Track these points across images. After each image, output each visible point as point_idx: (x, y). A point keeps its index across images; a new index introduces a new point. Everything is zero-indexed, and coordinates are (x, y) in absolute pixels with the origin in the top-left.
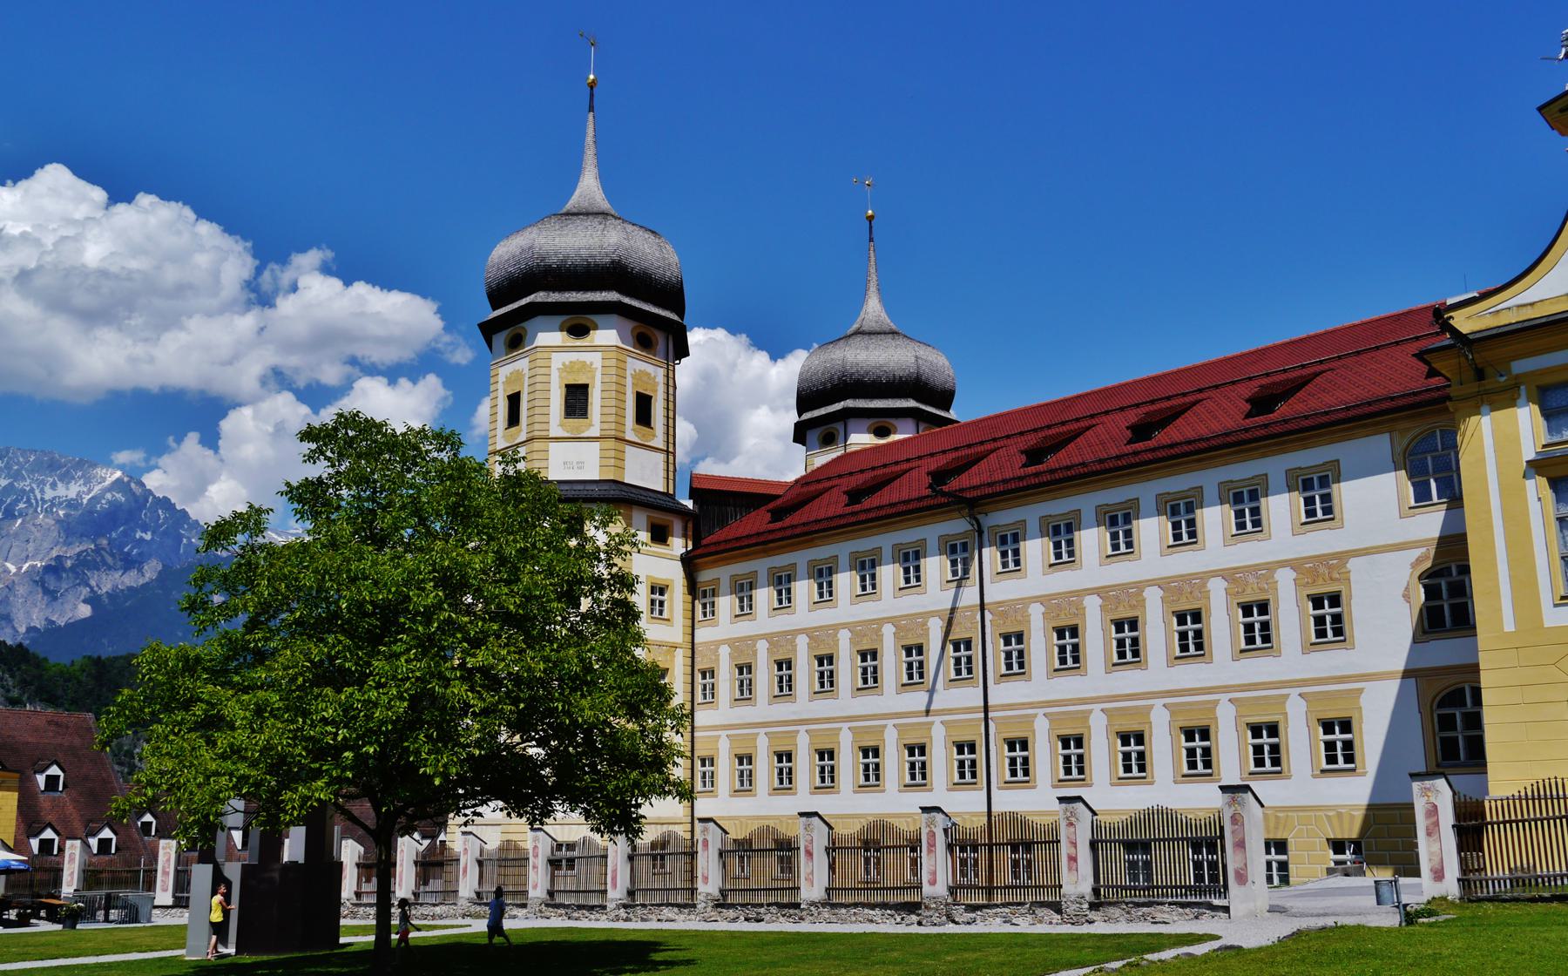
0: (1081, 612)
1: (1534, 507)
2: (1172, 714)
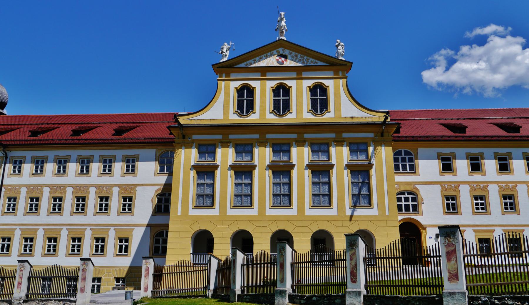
0: (41, 192)
1: (192, 179)
2: (69, 232)
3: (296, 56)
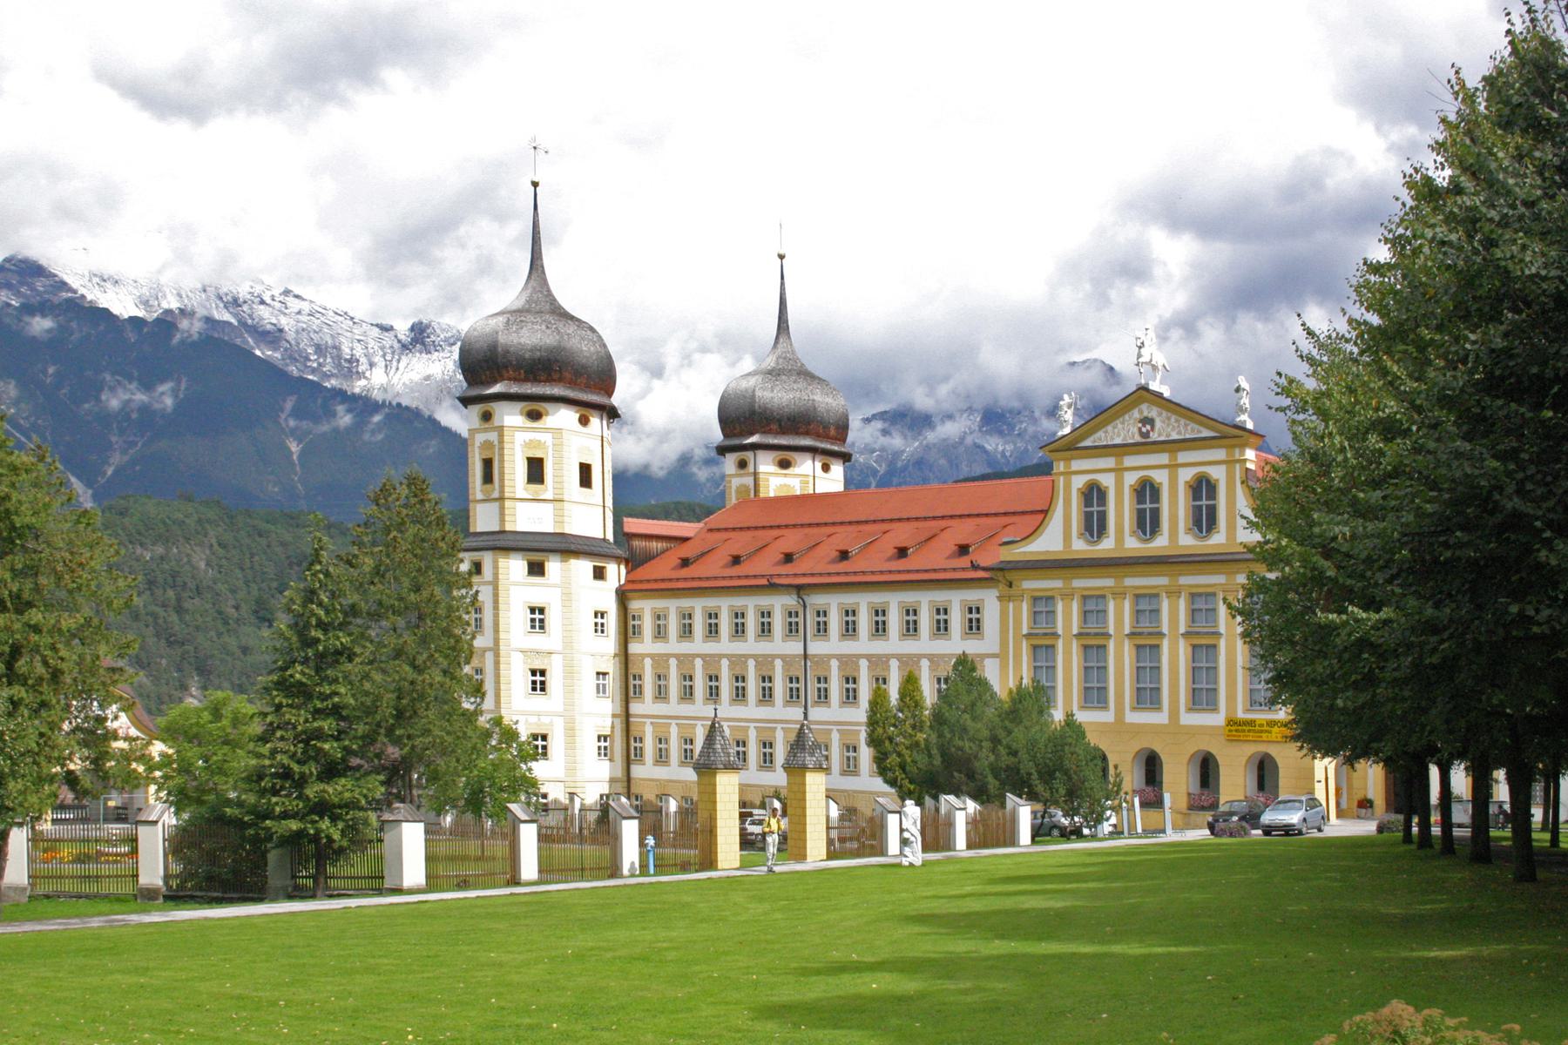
3: (1169, 419)
